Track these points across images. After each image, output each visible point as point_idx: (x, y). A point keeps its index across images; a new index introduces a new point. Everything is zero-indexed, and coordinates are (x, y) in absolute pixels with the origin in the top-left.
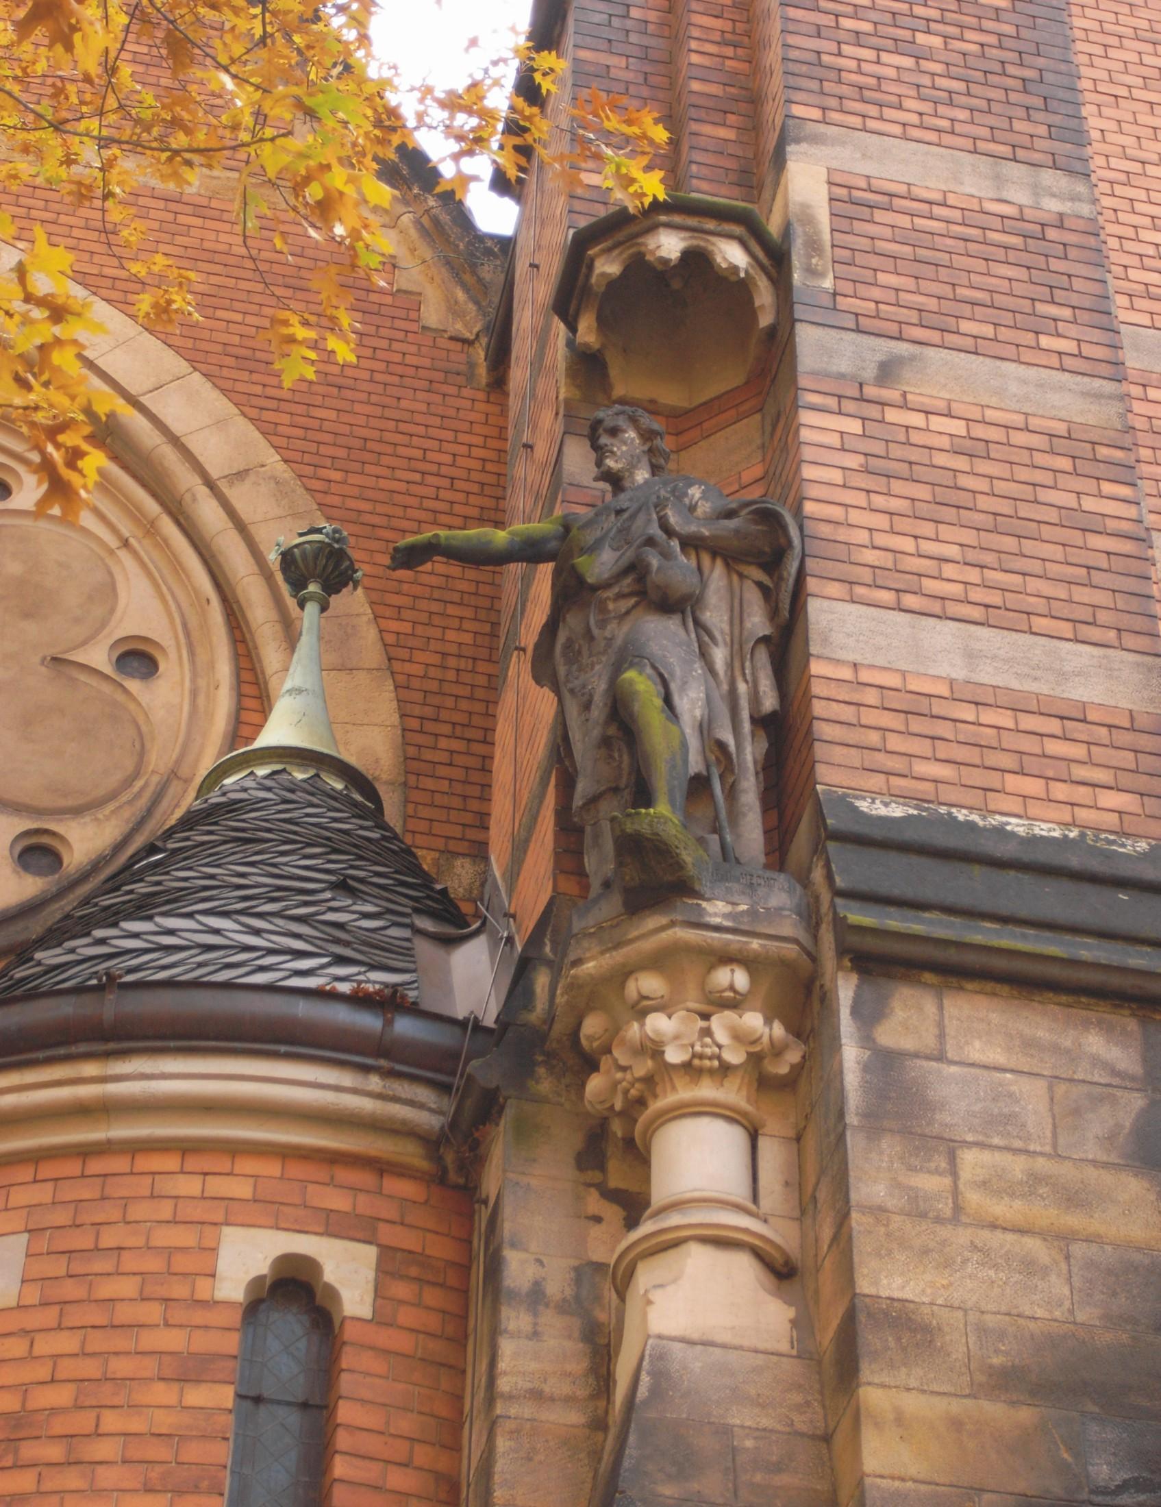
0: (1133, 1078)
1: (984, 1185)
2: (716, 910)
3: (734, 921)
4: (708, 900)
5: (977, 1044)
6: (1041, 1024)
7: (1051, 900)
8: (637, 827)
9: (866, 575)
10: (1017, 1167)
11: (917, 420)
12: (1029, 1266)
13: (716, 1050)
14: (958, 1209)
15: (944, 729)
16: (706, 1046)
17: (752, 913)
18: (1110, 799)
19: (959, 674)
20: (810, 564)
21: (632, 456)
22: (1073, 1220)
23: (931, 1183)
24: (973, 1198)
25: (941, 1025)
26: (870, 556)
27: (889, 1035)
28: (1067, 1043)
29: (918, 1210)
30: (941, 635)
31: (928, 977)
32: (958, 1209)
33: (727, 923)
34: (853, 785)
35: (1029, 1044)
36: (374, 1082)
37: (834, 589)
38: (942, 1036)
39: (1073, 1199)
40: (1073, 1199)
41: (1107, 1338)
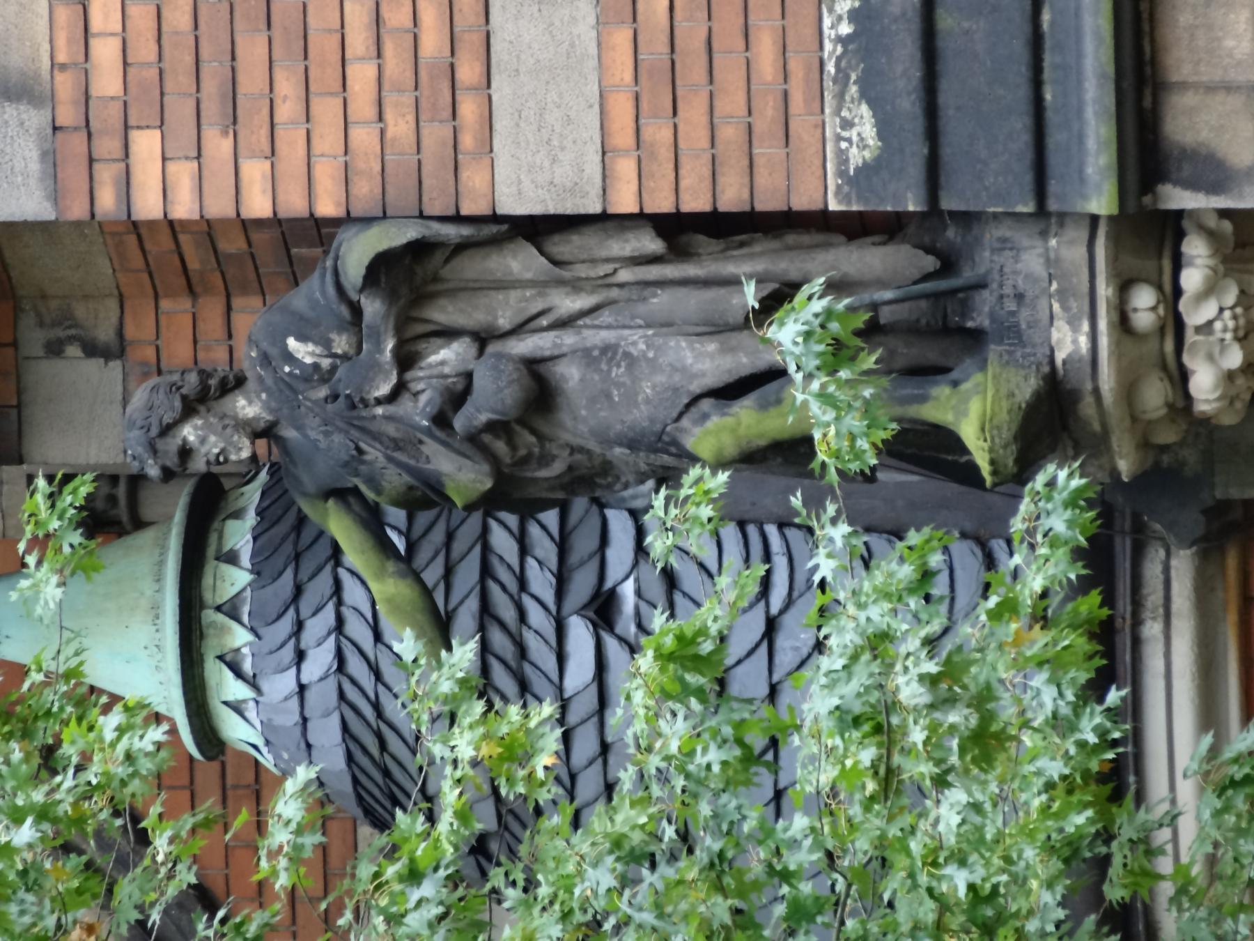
2: (1067, 341)
3: (1080, 319)
4: (1052, 351)
5: (1230, 43)
8: (1010, 462)
9: (436, 134)
11: (106, 52)
13: (1227, 314)
16: (1225, 330)
17: (1062, 295)
20: (436, 206)
21: (225, 427)
25: (1211, 89)
26: (400, 126)
31: (1147, 102)
33: (1086, 327)
34: (818, 162)
36: (1152, 629)
37: (474, 177)
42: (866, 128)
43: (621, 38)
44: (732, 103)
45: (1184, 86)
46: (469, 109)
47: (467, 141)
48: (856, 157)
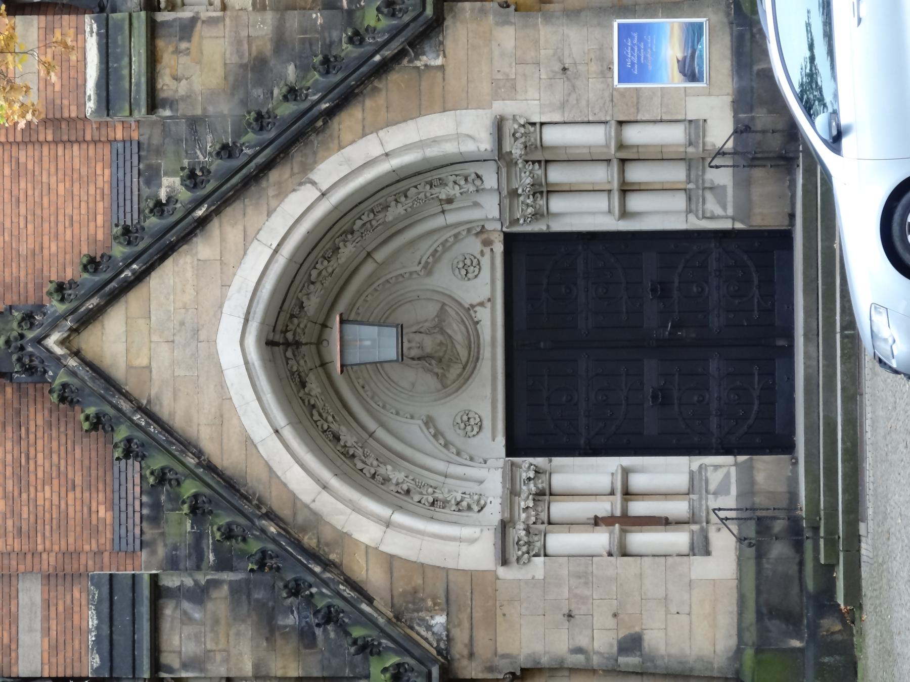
0: (177, 604)
1: (217, 644)
6: (166, 626)
7: (123, 618)
10: (210, 635)
12: (238, 634)
14: (224, 651)
15: (61, 640)
18: (76, 594)
19: (39, 635)
20: (6, 675)
22: (223, 622)
23: (219, 657)
24: (220, 647)
25: (171, 652)
27: (176, 664)
28: (169, 619)
29: (227, 660)
30: (24, 638)
32: (224, 651)
35: (172, 629)
37: (14, 669)
38: (174, 652)
39: (216, 622)
40: (216, 622)
41: (254, 617)
42: (97, 659)
43: (46, 640)
44: (69, 654)
45: (165, 651)
46: (13, 654)
47: (13, 661)
48: (95, 666)
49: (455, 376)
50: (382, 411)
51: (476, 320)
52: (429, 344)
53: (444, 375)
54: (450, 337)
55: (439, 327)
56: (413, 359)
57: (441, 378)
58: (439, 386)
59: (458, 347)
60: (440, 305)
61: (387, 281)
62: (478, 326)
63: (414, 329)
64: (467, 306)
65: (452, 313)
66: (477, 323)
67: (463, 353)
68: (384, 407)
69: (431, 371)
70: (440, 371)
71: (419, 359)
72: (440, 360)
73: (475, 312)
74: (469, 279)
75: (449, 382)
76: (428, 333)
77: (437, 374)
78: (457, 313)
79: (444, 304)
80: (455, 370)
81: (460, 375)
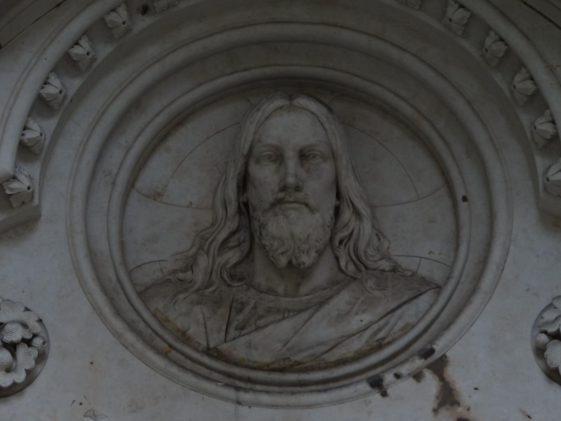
49: (180, 323)
50: (54, 51)
51: (389, 378)
52: (297, 228)
53: (183, 285)
54: (321, 304)
55: (359, 267)
56: (244, 182)
57: (175, 283)
58: (146, 277)
59: (286, 327)
60: (438, 276)
61: (521, 65)
62: (364, 387)
63: (350, 185)
64: (438, 347)
65: (410, 313)
66: (377, 384)
67: (268, 341)
68: (67, 64)
69: (202, 242)
70: (199, 277)
71: (245, 209)
72: (237, 275)
73: (418, 376)
74: (540, 352)
75: (159, 304)
76: (335, 240)
77: (190, 267)
78: (406, 329)
79: (439, 288)
80: (198, 321)
81: (184, 337)
